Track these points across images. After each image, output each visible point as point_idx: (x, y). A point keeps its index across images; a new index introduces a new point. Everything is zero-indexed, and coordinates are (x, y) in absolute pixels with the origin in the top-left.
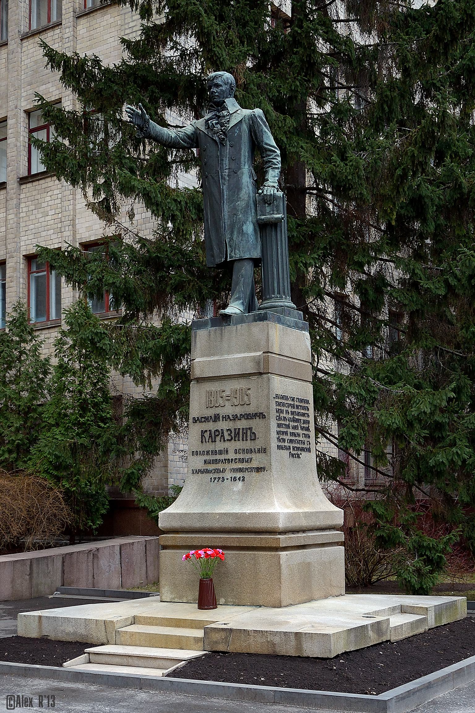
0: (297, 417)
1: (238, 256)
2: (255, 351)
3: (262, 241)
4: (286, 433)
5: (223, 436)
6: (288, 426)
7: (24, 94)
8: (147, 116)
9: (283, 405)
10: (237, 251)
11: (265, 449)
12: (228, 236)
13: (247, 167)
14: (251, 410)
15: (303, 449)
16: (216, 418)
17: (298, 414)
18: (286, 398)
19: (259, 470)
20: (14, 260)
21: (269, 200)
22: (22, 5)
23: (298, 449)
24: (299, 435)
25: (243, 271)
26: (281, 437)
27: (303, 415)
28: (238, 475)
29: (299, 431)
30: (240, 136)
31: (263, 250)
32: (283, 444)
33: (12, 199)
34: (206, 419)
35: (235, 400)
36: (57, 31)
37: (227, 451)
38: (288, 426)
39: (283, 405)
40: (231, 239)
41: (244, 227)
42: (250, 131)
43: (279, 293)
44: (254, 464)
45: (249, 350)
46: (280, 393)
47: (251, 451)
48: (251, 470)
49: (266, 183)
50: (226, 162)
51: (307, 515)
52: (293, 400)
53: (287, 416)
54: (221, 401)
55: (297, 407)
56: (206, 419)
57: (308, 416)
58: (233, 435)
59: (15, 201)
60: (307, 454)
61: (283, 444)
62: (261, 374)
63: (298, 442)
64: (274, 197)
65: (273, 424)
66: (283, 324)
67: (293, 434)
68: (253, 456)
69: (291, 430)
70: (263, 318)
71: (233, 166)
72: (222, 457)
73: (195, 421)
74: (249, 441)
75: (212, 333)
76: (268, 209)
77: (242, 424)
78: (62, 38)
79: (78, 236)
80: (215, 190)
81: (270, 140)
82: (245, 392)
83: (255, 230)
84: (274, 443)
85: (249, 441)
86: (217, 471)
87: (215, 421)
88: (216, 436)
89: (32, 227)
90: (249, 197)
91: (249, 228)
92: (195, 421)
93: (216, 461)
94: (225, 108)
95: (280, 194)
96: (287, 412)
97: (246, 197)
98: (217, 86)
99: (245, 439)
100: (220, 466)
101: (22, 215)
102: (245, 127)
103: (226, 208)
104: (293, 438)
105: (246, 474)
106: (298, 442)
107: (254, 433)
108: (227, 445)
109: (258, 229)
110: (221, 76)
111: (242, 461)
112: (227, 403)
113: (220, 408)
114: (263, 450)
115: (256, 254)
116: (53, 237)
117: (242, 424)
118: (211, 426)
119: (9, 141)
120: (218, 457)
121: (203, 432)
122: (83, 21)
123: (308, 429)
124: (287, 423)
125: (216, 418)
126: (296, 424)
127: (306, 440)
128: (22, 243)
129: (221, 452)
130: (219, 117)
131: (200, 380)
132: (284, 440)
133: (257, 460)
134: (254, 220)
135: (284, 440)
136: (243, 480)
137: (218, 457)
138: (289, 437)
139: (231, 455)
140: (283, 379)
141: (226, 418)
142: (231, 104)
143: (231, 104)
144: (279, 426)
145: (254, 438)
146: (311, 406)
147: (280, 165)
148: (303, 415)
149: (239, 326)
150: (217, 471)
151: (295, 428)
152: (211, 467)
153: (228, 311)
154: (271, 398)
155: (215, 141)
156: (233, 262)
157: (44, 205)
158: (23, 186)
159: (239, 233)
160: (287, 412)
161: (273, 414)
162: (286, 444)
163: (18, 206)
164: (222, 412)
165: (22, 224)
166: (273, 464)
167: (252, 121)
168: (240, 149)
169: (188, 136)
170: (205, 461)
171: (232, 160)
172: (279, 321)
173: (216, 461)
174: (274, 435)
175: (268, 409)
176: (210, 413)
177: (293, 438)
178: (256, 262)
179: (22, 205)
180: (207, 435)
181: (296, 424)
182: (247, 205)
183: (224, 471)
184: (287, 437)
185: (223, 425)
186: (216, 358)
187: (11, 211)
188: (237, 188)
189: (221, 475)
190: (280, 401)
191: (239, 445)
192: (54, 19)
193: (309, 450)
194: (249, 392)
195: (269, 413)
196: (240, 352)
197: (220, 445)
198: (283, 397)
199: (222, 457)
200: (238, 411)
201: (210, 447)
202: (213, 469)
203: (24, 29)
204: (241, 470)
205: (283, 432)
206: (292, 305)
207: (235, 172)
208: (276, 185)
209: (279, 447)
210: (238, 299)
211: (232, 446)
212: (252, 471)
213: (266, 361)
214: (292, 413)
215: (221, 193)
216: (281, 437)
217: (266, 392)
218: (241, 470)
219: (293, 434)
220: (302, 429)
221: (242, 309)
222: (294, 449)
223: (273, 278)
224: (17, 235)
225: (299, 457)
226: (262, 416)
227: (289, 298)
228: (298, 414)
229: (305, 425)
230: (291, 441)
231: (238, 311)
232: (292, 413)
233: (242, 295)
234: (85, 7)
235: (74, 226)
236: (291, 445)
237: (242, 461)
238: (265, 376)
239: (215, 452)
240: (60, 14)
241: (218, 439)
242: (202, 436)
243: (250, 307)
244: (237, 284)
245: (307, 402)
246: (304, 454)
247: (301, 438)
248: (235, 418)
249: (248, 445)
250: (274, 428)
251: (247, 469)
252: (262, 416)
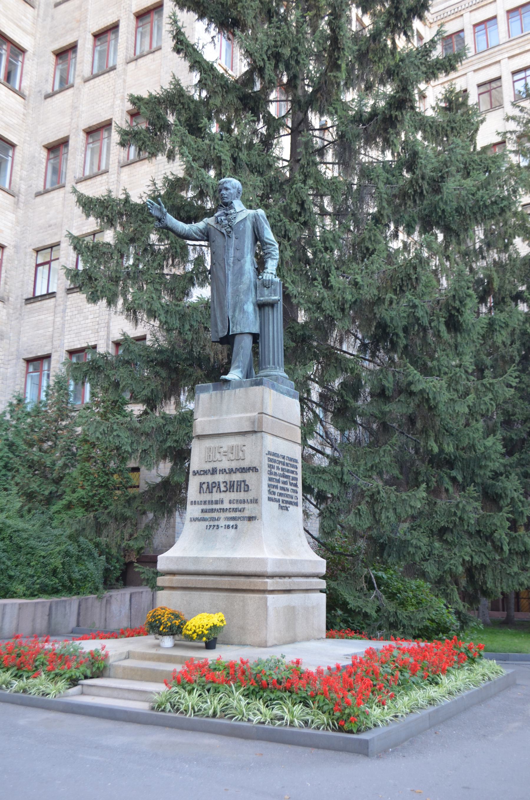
0: (286, 474)
1: (239, 331)
2: (251, 412)
3: (261, 320)
4: (277, 487)
5: (219, 487)
6: (278, 481)
7: (75, 224)
8: (165, 210)
9: (275, 461)
10: (238, 327)
11: (257, 500)
12: (230, 314)
13: (249, 256)
14: (245, 464)
15: (291, 503)
16: (214, 471)
17: (288, 471)
19: (250, 519)
20: (58, 354)
21: (267, 285)
22: (79, 157)
23: (287, 502)
24: (288, 490)
25: (243, 344)
26: (272, 490)
27: (292, 472)
28: (231, 523)
29: (288, 486)
30: (244, 231)
31: (262, 326)
32: (273, 496)
33: (59, 305)
34: (205, 472)
35: (231, 455)
36: (105, 177)
37: (222, 502)
38: (278, 481)
39: (275, 461)
40: (233, 316)
41: (245, 307)
42: (253, 228)
43: (274, 364)
44: (247, 514)
45: (245, 410)
46: (272, 450)
47: (244, 502)
48: (243, 518)
49: (266, 271)
50: (232, 251)
51: (294, 562)
52: (284, 458)
53: (278, 472)
54: (218, 456)
55: (287, 465)
56: (205, 472)
57: (297, 474)
58: (228, 486)
59: (62, 307)
60: (295, 507)
61: (273, 496)
62: (255, 432)
63: (287, 496)
64: (272, 282)
65: (265, 477)
66: (276, 390)
67: (282, 489)
68: (246, 506)
69: (280, 485)
70: (259, 383)
71: (238, 254)
72: (218, 507)
73: (195, 473)
74: (242, 493)
75: (213, 396)
76: (266, 291)
77: (237, 477)
78: (108, 182)
79: (111, 336)
80: (221, 275)
81: (269, 235)
82: (241, 449)
83: (255, 310)
84: (265, 495)
85: (242, 493)
86: (213, 519)
87: (212, 474)
88: (213, 487)
89: (74, 328)
90: (250, 281)
91: (250, 308)
92: (195, 473)
93: (212, 511)
94: (232, 208)
95: (278, 279)
96: (278, 468)
97: (248, 281)
98: (227, 189)
99: (239, 490)
100: (215, 515)
101: (67, 318)
102: (249, 224)
103: (230, 290)
104: (283, 492)
105: (239, 523)
106: (287, 496)
107: (248, 486)
108: (222, 496)
109: (257, 309)
110: (230, 182)
111: (235, 510)
112: (224, 458)
113: (217, 463)
114: (255, 501)
115: (255, 330)
116: (91, 336)
117: (237, 477)
118: (209, 479)
119: (60, 260)
120: (214, 506)
121: (201, 484)
122: (126, 169)
123: (296, 485)
124: (278, 478)
125: (214, 471)
126: (285, 480)
127: (294, 495)
128: (66, 341)
129: (216, 502)
130: (227, 214)
131: (199, 437)
132: (274, 493)
133: (249, 510)
134: (254, 301)
135: (274, 493)
136: (236, 528)
137: (214, 506)
139: (226, 505)
140: (275, 438)
141: (223, 471)
142: (238, 205)
143: (238, 205)
144: (270, 479)
145: (247, 489)
146: (299, 465)
147: (278, 257)
148: (292, 472)
149: (237, 390)
150: (213, 519)
151: (285, 483)
152: (207, 515)
153: (228, 377)
154: (264, 454)
155: (223, 233)
156: (234, 336)
157: (85, 310)
158: (70, 296)
159: (240, 311)
160: (278, 468)
161: (265, 469)
162: (276, 497)
163: (64, 311)
164: (219, 466)
165: (67, 326)
166: (263, 513)
167: (256, 218)
168: (244, 242)
169: (201, 231)
170: (202, 511)
171: (237, 249)
172: (273, 387)
173: (212, 511)
174: (265, 488)
175: (261, 463)
176: (208, 466)
177: (283, 492)
178: (256, 337)
179: (68, 311)
180: (205, 486)
181: (285, 480)
182: (249, 288)
183: (218, 519)
184: (278, 491)
185: (220, 478)
186: (215, 418)
187: (58, 315)
188: (240, 273)
189: (216, 523)
190: (271, 457)
191: (234, 496)
192: (103, 167)
193: (296, 504)
194: (244, 448)
195: (261, 467)
196: (238, 413)
197: (216, 496)
198: (274, 454)
199: (218, 507)
200: (234, 465)
201: (207, 497)
202: (210, 518)
203: (79, 175)
204: (234, 519)
206: (285, 375)
207: (239, 260)
208: (274, 272)
209: (270, 499)
210: (238, 367)
211: (227, 497)
212: (244, 520)
213: (260, 421)
214: (283, 470)
215: (226, 276)
216: (272, 490)
217: (259, 448)
218: (234, 519)
219: (282, 489)
220: (291, 484)
221: (241, 376)
223: (269, 351)
224: (62, 334)
225: (287, 509)
226: (255, 470)
227: (282, 369)
228: (288, 471)
229: (294, 482)
230: (281, 495)
231: (237, 378)
232: (283, 470)
233: (241, 364)
234: (128, 159)
235: (108, 327)
236: (281, 498)
237: (235, 510)
238: (259, 435)
239: (211, 502)
240: (107, 164)
241: (215, 490)
242: (201, 487)
243: (248, 375)
244: (238, 354)
245: (296, 461)
246: (291, 508)
247: (289, 493)
248: (231, 471)
249: (242, 495)
250: (265, 482)
251: (239, 518)
252: (255, 470)
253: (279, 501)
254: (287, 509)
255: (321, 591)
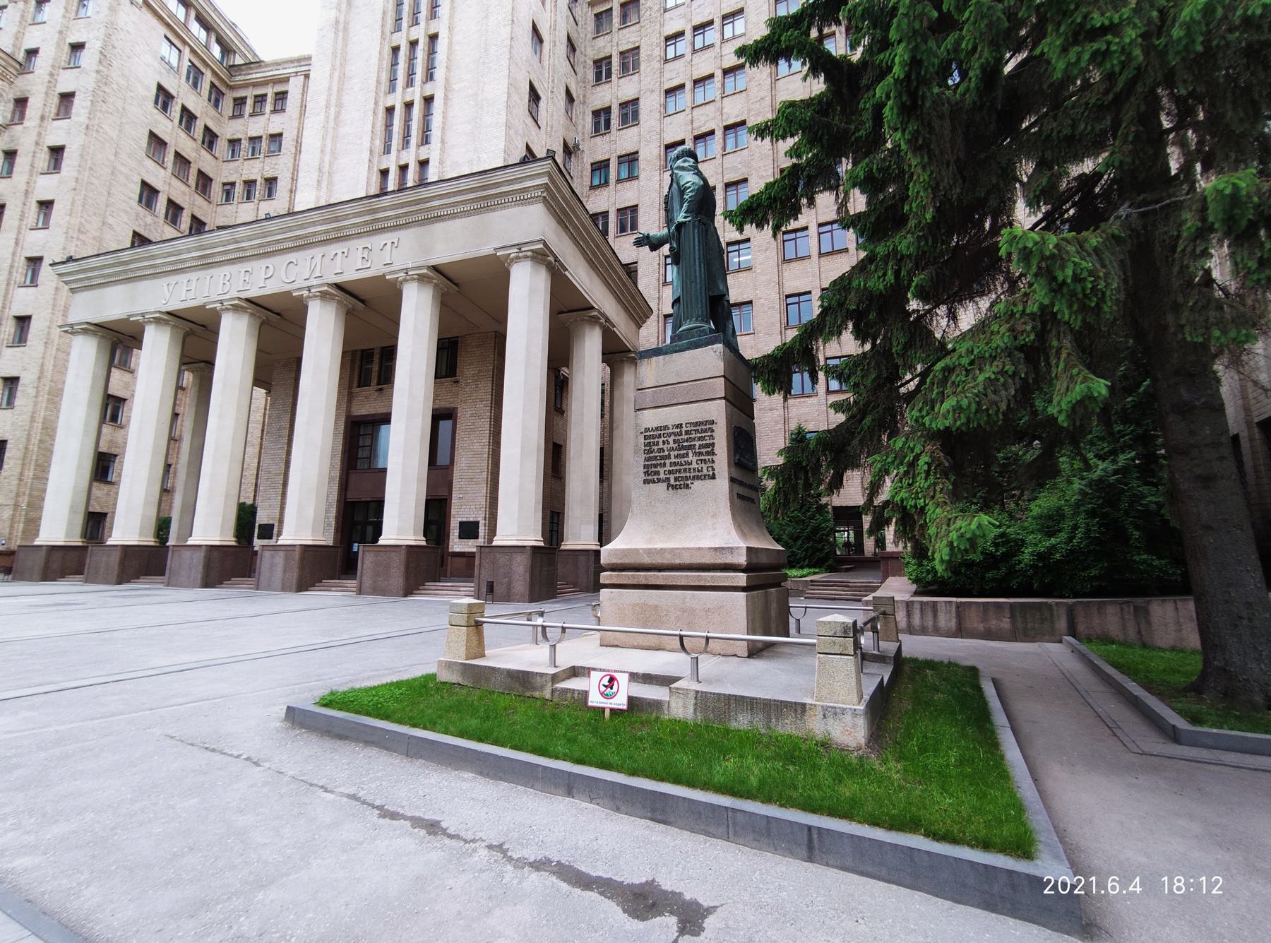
6: (668, 457)
15: (699, 478)
18: (666, 427)
55: (687, 433)
67: (674, 464)
138: (668, 467)
144: (647, 460)
162: (662, 476)
193: (713, 477)
205: (656, 466)
222: (676, 479)
230: (670, 472)
253: (668, 479)
254: (687, 487)
255: (743, 589)
